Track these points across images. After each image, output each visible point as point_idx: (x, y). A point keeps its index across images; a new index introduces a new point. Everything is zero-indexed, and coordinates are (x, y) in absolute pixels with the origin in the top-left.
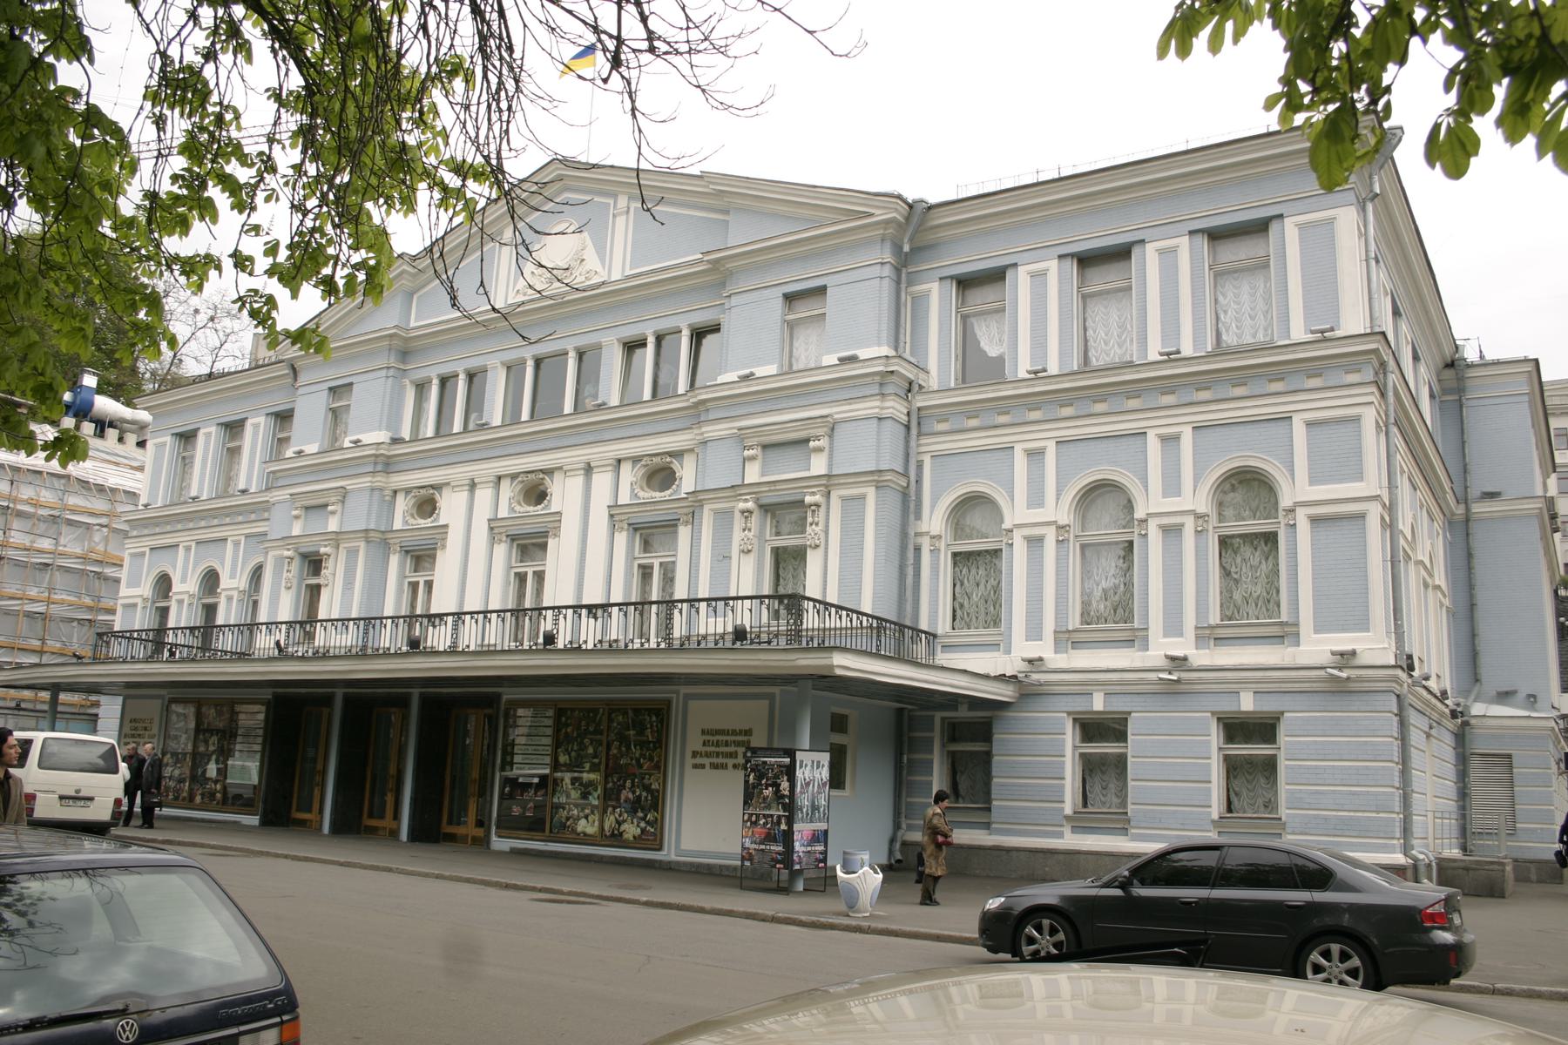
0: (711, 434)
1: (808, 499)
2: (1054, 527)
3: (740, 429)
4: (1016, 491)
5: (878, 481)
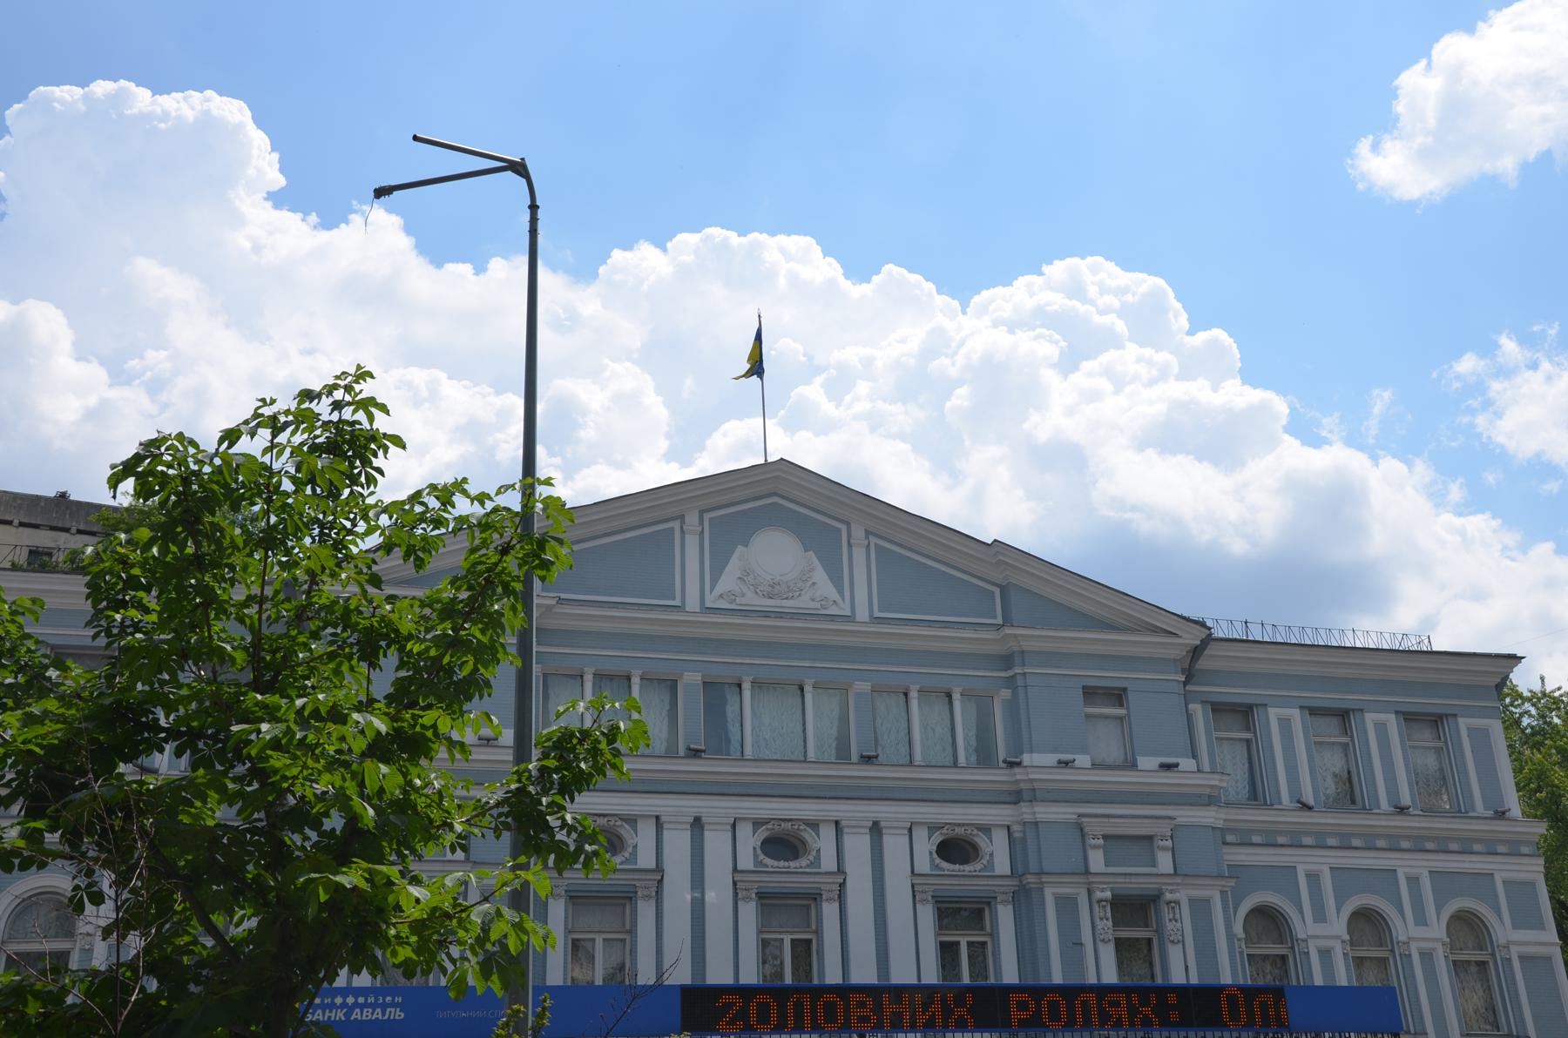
0: (1044, 816)
1: (1168, 896)
2: (1339, 941)
3: (1080, 816)
4: (1406, 912)
5: (1224, 886)
